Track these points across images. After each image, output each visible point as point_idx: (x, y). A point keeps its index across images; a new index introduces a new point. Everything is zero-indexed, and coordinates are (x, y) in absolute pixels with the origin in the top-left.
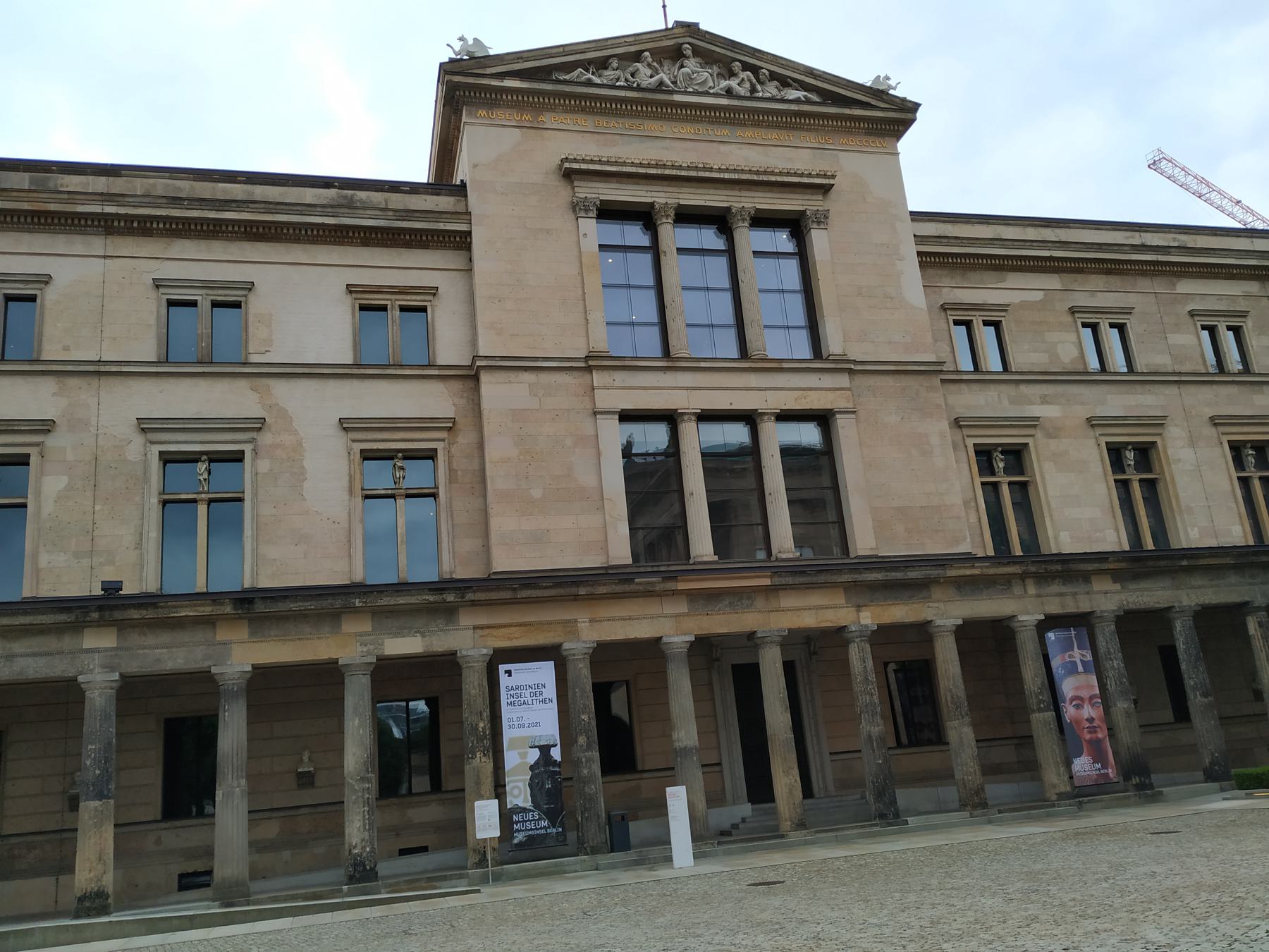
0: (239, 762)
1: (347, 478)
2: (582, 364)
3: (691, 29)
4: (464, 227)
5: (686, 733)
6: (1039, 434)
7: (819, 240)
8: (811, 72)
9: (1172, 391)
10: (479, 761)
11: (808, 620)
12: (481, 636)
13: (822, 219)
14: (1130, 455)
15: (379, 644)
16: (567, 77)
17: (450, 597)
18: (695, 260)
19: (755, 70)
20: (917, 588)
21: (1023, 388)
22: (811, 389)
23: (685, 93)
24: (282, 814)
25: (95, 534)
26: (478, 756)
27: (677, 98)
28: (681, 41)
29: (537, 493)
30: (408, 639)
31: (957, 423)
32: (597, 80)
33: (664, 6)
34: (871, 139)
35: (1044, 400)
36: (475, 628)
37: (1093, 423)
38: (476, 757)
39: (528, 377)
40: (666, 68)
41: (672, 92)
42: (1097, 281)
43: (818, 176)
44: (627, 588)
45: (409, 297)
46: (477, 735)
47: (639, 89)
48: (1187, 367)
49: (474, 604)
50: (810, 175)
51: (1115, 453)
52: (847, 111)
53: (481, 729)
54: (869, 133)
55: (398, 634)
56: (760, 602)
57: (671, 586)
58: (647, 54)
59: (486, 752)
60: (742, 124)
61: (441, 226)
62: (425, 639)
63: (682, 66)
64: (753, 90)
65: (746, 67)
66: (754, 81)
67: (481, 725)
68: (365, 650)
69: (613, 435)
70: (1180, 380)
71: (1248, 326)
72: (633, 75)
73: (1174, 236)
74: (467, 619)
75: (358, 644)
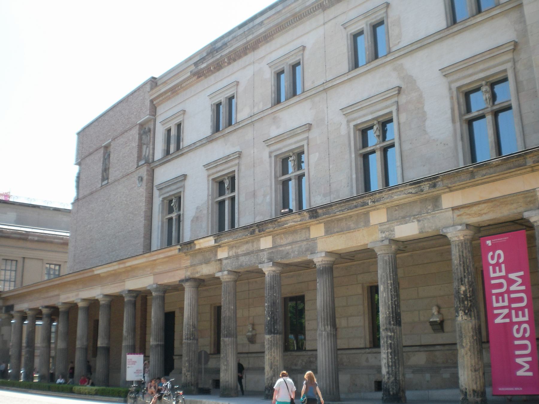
0: (326, 314)
1: (449, 112)
10: (461, 318)
12: (458, 216)
15: (392, 231)
24: (426, 349)
25: (331, 182)
26: (460, 314)
30: (409, 225)
36: (454, 209)
38: (459, 315)
46: (459, 297)
53: (462, 292)
59: (466, 311)
62: (420, 223)
67: (463, 288)
68: (384, 235)
75: (380, 232)
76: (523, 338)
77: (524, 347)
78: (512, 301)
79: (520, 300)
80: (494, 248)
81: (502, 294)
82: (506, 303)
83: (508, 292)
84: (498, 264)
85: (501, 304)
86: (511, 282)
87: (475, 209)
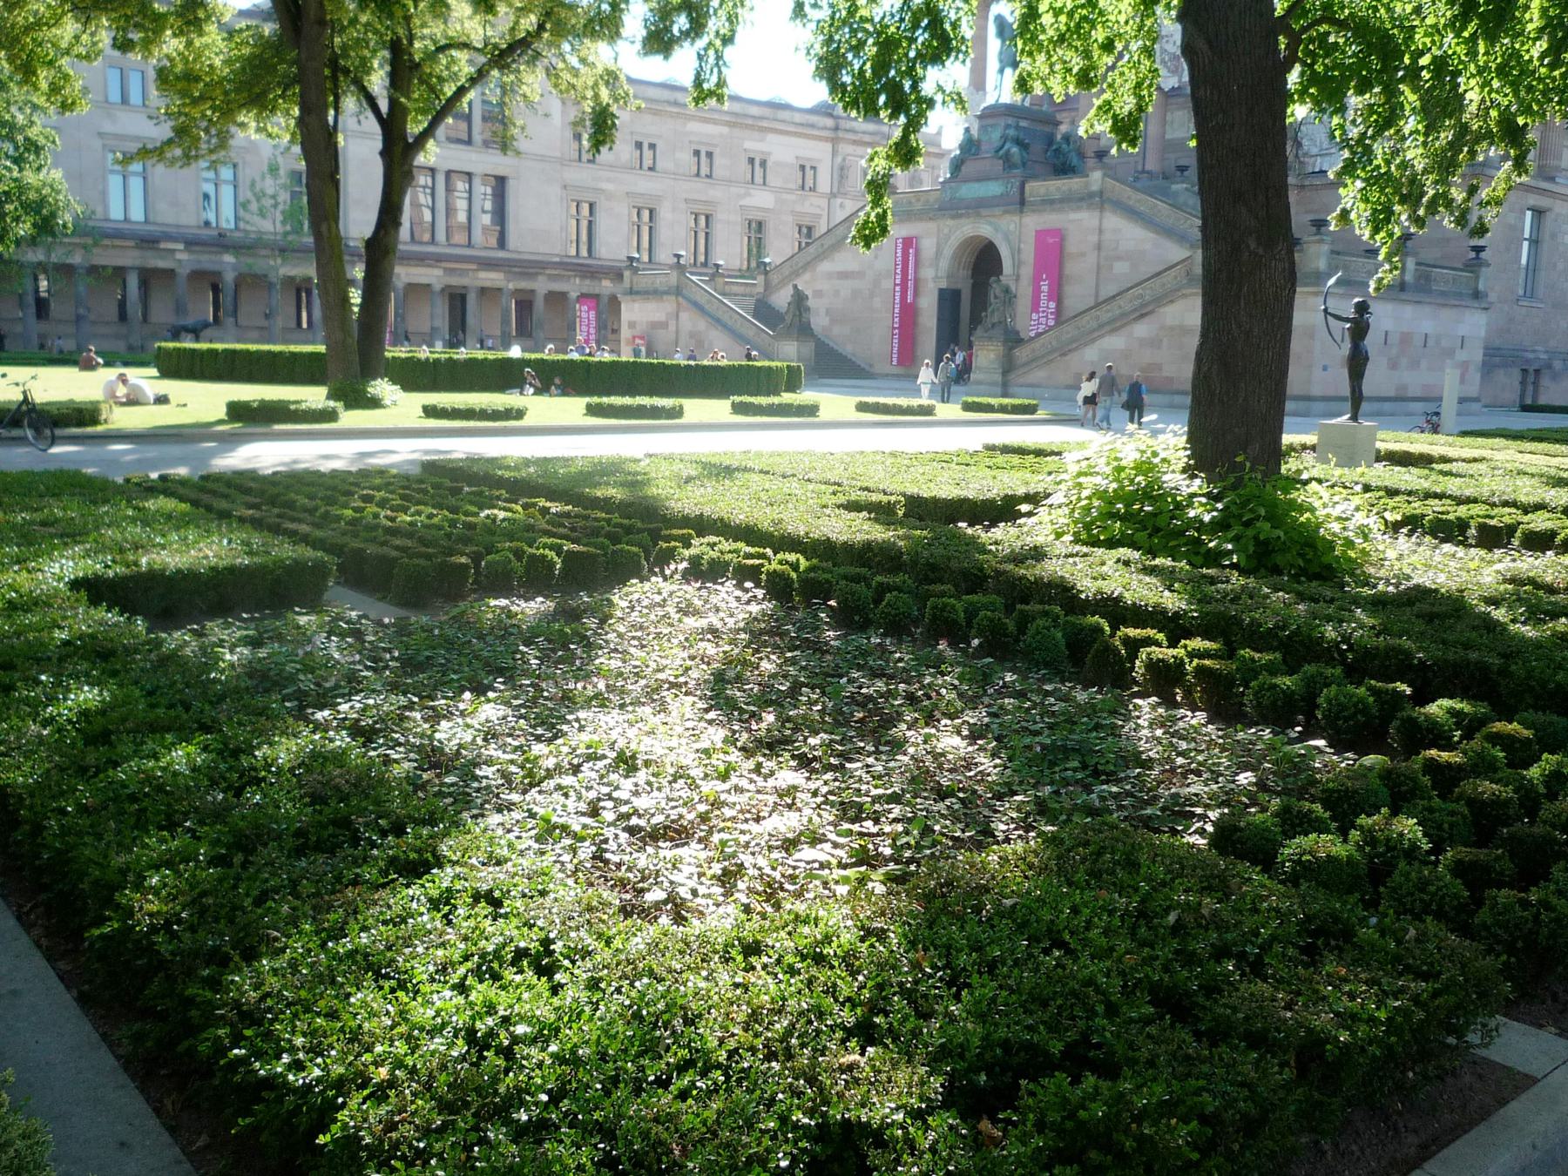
11: (488, 284)
20: (531, 276)
31: (565, 187)
35: (609, 180)
71: (717, 152)
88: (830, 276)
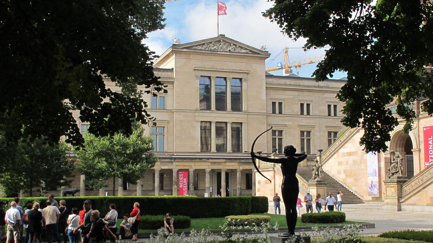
2: (194, 111)
3: (223, 36)
4: (173, 81)
5: (207, 185)
6: (286, 128)
7: (244, 84)
8: (248, 46)
9: (318, 119)
11: (231, 168)
13: (247, 80)
14: (305, 133)
16: (196, 48)
17: (173, 160)
18: (219, 79)
19: (236, 45)
21: (285, 118)
22: (239, 118)
23: (220, 51)
27: (219, 53)
28: (220, 39)
29: (184, 137)
32: (202, 48)
33: (218, 24)
34: (260, 60)
35: (289, 121)
36: (176, 165)
37: (300, 126)
39: (183, 113)
40: (217, 44)
41: (218, 51)
42: (306, 93)
43: (246, 71)
44: (201, 160)
45: (161, 95)
47: (211, 50)
48: (322, 114)
49: (176, 161)
50: (245, 71)
51: (302, 133)
52: (255, 55)
54: (259, 59)
55: (164, 165)
56: (223, 164)
57: (208, 161)
58: (213, 42)
60: (232, 57)
61: (169, 80)
63: (220, 44)
64: (235, 49)
65: (234, 45)
66: (235, 48)
69: (199, 125)
70: (320, 117)
72: (210, 46)
73: (325, 83)
74: (174, 164)
76: (185, 190)
77: (185, 192)
78: (183, 184)
79: (185, 184)
80: (181, 174)
81: (182, 182)
82: (182, 184)
83: (183, 182)
84: (181, 177)
85: (181, 184)
86: (184, 180)
87: (180, 166)
88: (344, 154)
